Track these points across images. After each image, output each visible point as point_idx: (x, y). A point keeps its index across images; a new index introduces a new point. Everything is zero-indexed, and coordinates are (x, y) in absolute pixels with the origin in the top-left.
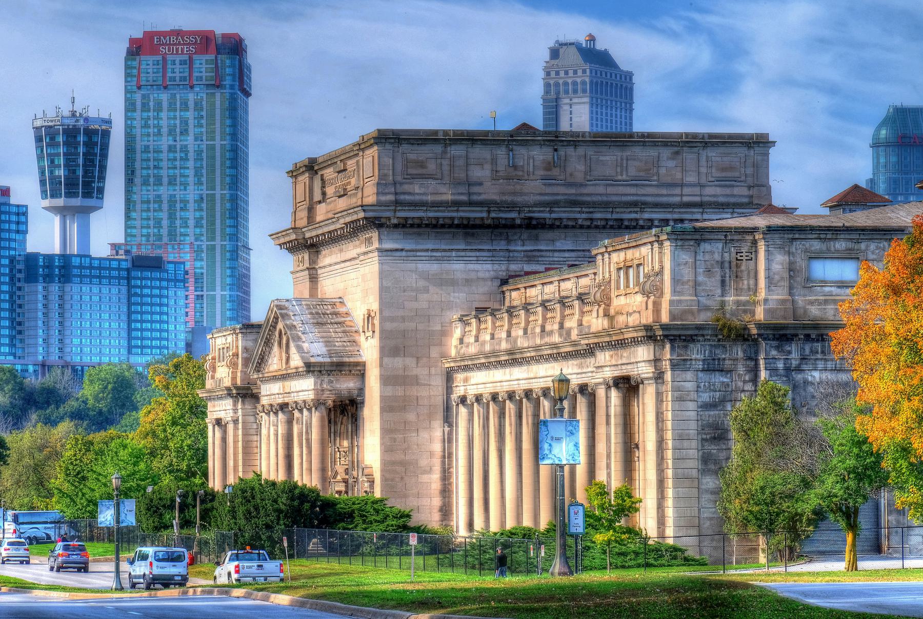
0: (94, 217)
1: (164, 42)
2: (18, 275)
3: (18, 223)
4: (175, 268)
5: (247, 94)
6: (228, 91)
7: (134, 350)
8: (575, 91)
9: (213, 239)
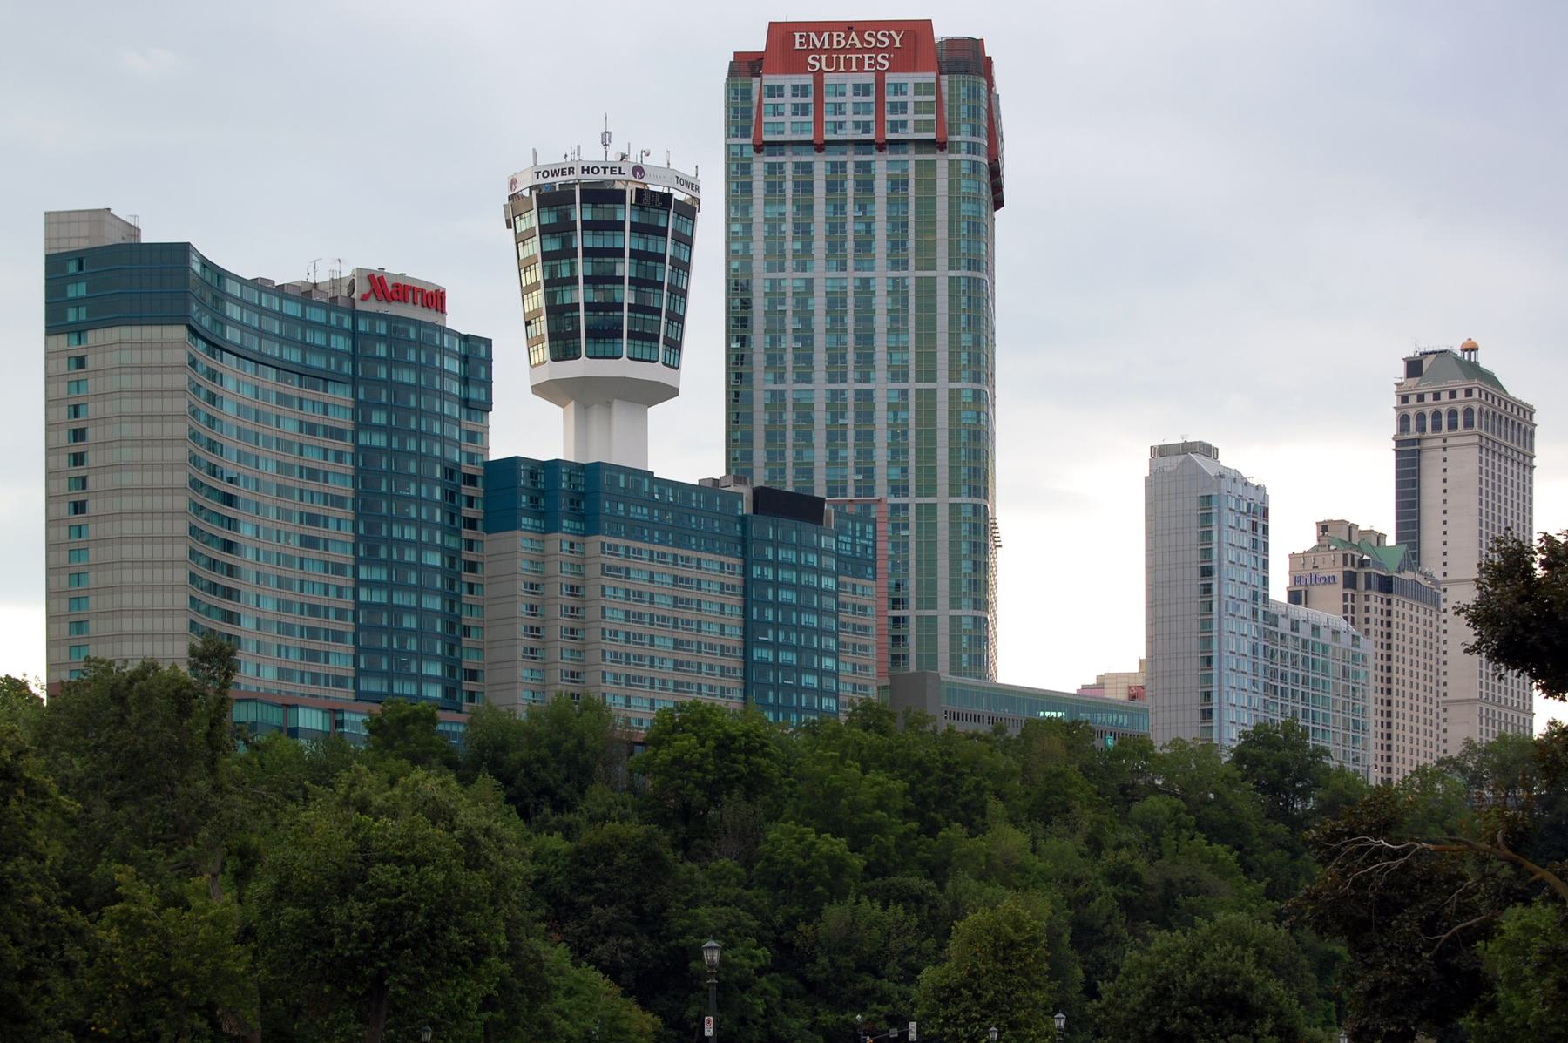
0: (654, 412)
1: (818, 45)
2: (466, 512)
3: (465, 381)
5: (998, 204)
8: (1453, 425)
9: (932, 491)
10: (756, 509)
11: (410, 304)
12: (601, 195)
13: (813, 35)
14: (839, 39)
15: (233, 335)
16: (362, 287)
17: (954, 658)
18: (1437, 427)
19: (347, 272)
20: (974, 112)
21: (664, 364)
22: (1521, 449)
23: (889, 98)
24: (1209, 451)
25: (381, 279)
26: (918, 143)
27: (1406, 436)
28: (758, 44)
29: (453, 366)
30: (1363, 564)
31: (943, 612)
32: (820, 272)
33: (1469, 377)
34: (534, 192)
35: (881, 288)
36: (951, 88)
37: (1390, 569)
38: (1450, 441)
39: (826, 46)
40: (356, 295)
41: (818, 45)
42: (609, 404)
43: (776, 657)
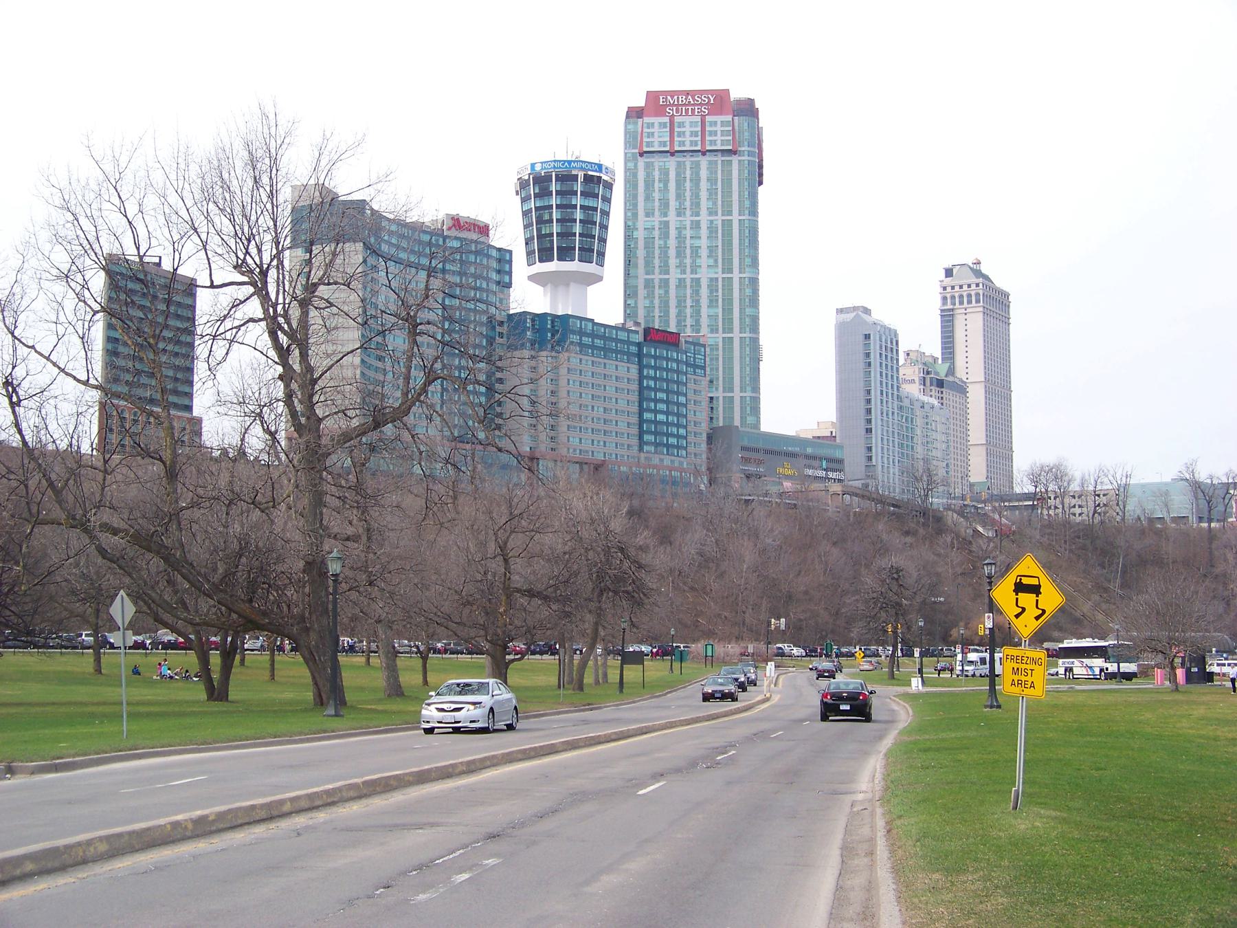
0: (592, 289)
1: (672, 102)
3: (499, 272)
4: (694, 350)
5: (761, 183)
6: (746, 158)
7: (646, 448)
8: (970, 302)
9: (731, 330)
10: (645, 340)
11: (472, 232)
12: (566, 178)
13: (669, 97)
14: (682, 99)
15: (385, 248)
16: (448, 223)
17: (743, 418)
18: (961, 303)
19: (441, 216)
20: (752, 135)
21: (597, 264)
22: (1003, 314)
23: (708, 129)
24: (867, 311)
25: (458, 219)
26: (722, 151)
27: (946, 308)
28: (640, 102)
29: (494, 265)
30: (928, 373)
31: (737, 394)
32: (672, 217)
33: (977, 277)
34: (531, 176)
35: (704, 225)
36: (739, 124)
37: (942, 376)
38: (968, 310)
39: (676, 103)
40: (445, 227)
41: (672, 102)
42: (568, 285)
43: (656, 417)
